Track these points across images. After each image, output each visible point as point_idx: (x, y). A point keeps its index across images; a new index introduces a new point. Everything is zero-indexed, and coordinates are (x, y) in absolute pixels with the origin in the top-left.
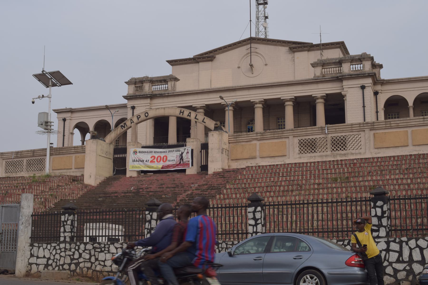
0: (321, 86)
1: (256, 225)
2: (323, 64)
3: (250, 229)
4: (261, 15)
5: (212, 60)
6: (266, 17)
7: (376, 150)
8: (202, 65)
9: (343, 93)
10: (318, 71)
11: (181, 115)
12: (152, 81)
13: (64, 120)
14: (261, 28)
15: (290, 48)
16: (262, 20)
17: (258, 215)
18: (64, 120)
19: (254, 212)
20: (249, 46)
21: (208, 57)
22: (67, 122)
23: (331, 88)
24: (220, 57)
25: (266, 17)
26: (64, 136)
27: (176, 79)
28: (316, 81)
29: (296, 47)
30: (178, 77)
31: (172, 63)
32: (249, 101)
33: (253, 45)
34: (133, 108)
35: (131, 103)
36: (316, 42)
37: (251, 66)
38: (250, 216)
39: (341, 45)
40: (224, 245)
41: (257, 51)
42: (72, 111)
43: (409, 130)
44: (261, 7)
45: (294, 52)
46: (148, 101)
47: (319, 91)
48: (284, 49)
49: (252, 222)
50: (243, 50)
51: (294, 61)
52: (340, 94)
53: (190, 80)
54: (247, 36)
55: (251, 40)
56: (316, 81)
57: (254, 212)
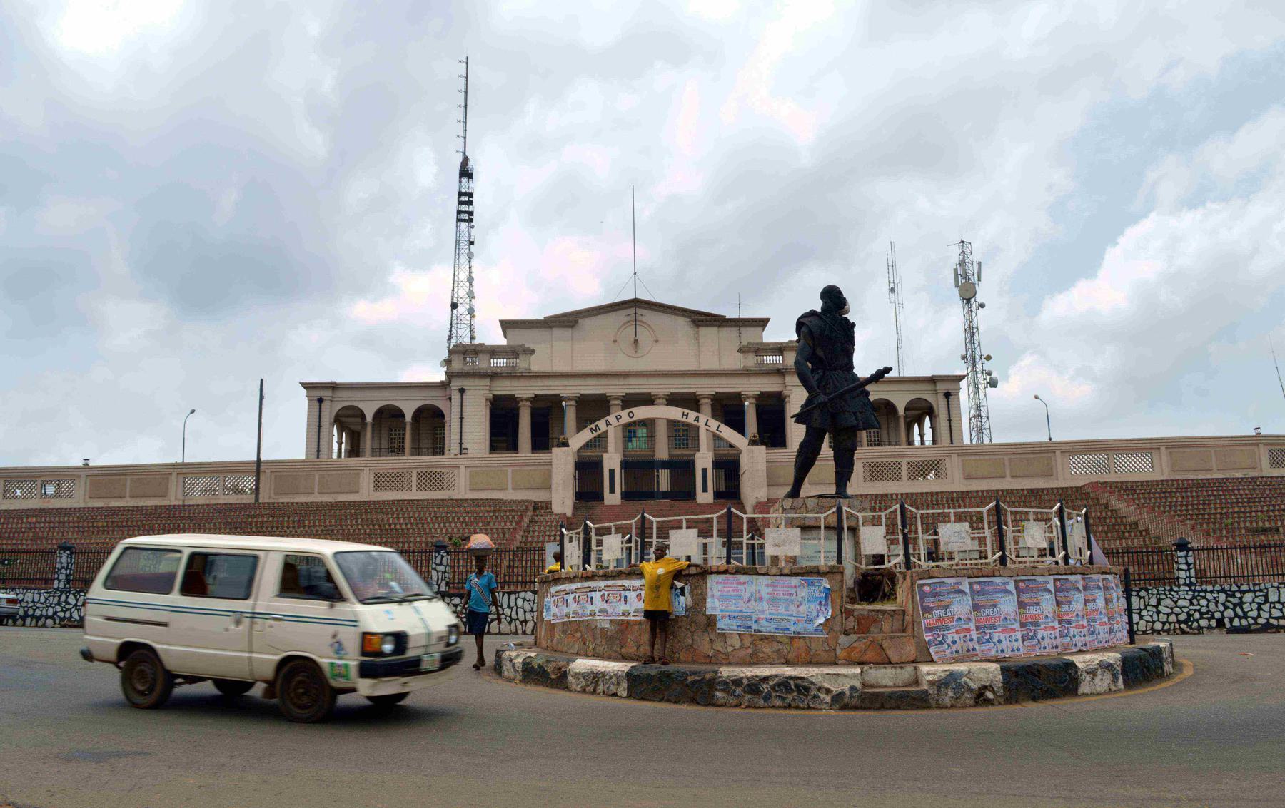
0: (753, 380)
1: (1189, 569)
2: (761, 349)
3: (1182, 574)
4: (465, 239)
5: (572, 327)
6: (472, 243)
7: (965, 482)
8: (557, 332)
9: (785, 392)
10: (750, 361)
11: (684, 419)
12: (494, 352)
13: (320, 400)
14: (463, 259)
15: (694, 322)
16: (464, 245)
17: (1191, 560)
18: (320, 400)
19: (1186, 556)
20: (632, 311)
21: (568, 321)
22: (326, 405)
23: (769, 385)
24: (586, 323)
25: (472, 243)
26: (320, 426)
27: (533, 352)
28: (746, 373)
29: (701, 319)
30: (532, 347)
31: (507, 326)
32: (649, 394)
33: (640, 311)
34: (462, 391)
35: (456, 384)
36: (731, 314)
37: (636, 341)
38: (1182, 560)
39: (763, 323)
40: (1155, 592)
41: (643, 319)
42: (334, 387)
43: (1006, 458)
44: (464, 225)
45: (698, 326)
46: (487, 382)
47: (751, 387)
48: (682, 321)
49: (1184, 567)
50: (621, 316)
51: (697, 339)
52: (780, 393)
53: (551, 356)
54: (630, 296)
55: (636, 303)
56: (746, 373)
57: (1186, 556)
